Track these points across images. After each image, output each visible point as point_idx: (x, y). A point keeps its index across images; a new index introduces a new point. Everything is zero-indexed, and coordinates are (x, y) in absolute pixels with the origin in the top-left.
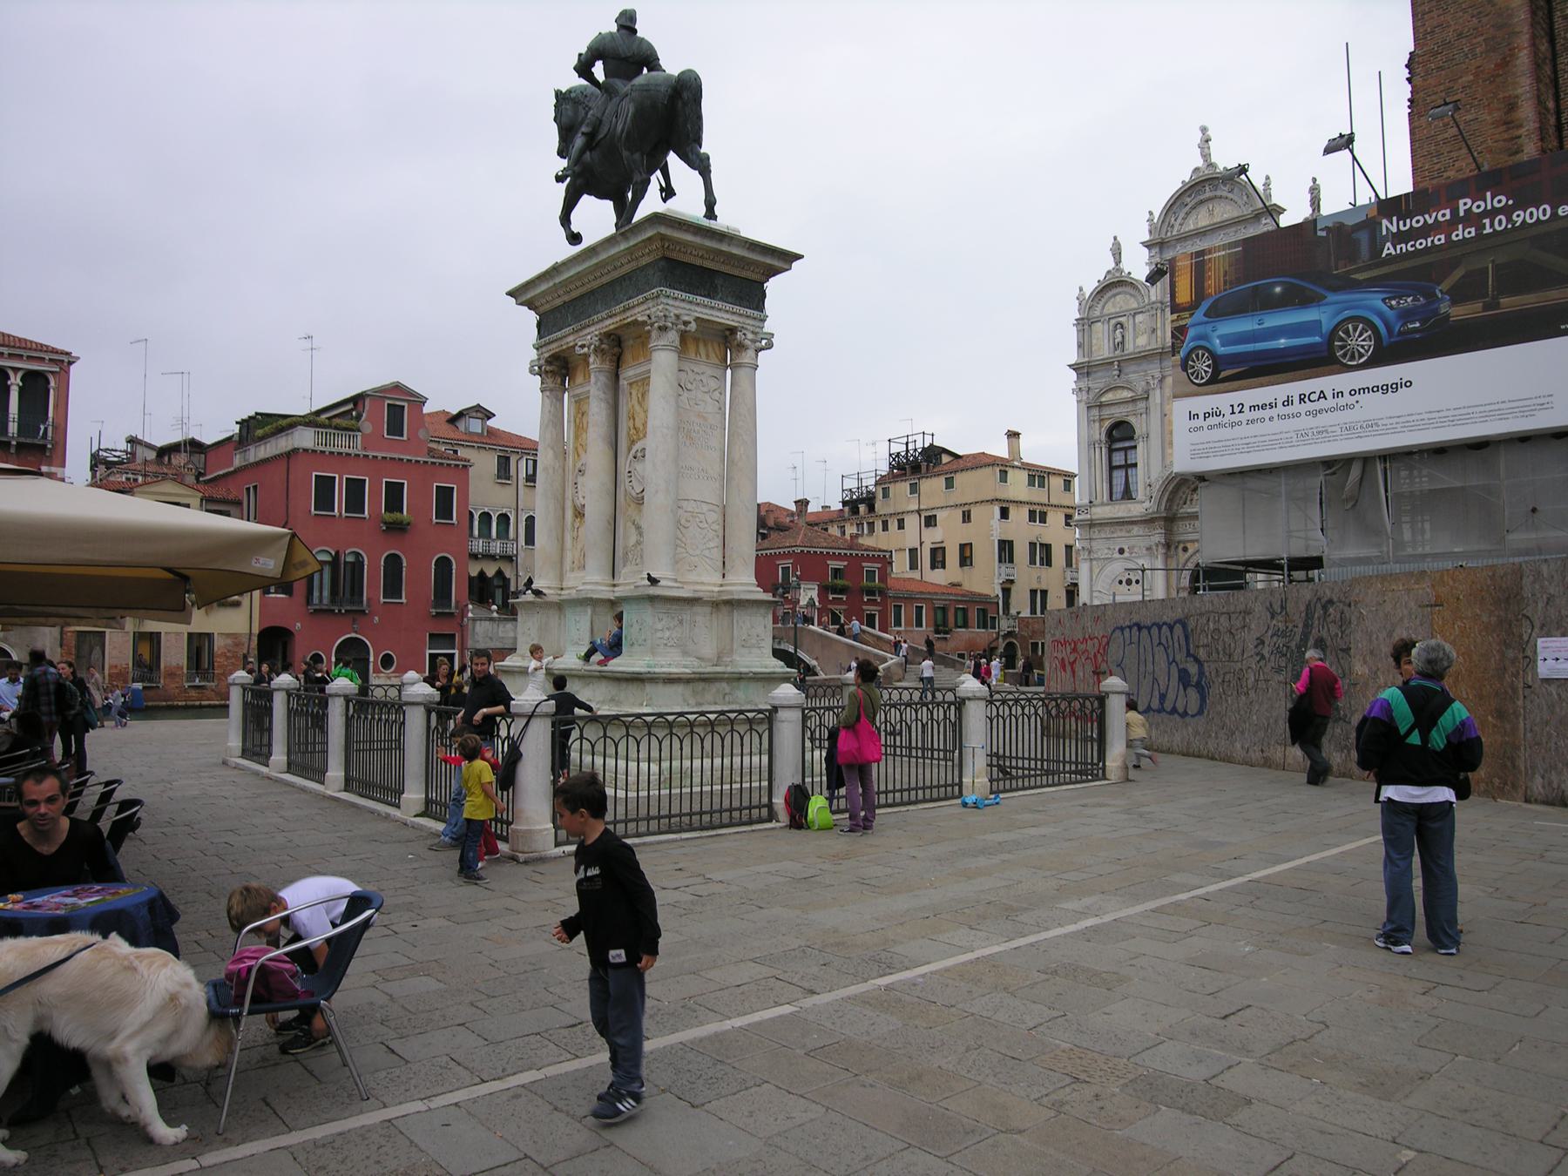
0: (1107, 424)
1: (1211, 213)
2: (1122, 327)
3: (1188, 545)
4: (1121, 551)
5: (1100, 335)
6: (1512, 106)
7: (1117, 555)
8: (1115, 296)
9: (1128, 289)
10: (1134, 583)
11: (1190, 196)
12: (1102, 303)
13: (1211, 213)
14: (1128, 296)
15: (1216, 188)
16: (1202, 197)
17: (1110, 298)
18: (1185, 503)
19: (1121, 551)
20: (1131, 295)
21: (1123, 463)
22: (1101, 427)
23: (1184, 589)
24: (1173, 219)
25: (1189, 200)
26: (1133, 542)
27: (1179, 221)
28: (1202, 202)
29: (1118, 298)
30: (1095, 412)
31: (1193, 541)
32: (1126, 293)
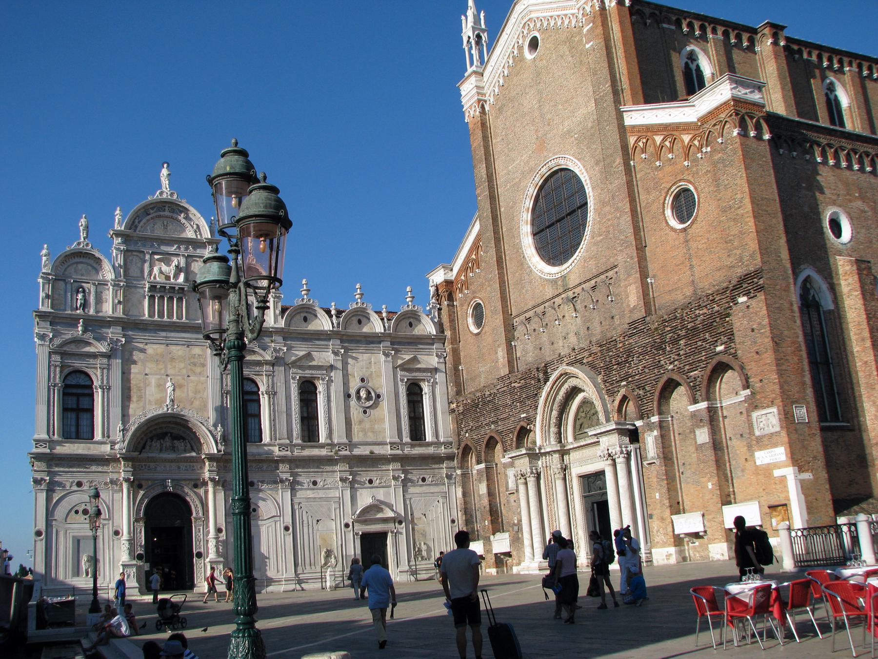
0: (66, 371)
1: (166, 227)
2: (84, 291)
3: (143, 483)
4: (79, 484)
5: (62, 292)
6: (792, 305)
7: (75, 488)
8: (77, 263)
9: (91, 262)
10: (80, 512)
11: (152, 209)
12: (67, 264)
13: (166, 227)
14: (90, 268)
15: (173, 211)
16: (162, 213)
17: (74, 263)
18: (144, 448)
19: (79, 484)
20: (91, 266)
21: (75, 406)
22: (61, 372)
23: (141, 519)
24: (137, 221)
25: (152, 211)
26: (91, 477)
27: (142, 224)
28: (160, 216)
29: (80, 266)
30: (57, 358)
31: (147, 480)
32: (88, 264)
